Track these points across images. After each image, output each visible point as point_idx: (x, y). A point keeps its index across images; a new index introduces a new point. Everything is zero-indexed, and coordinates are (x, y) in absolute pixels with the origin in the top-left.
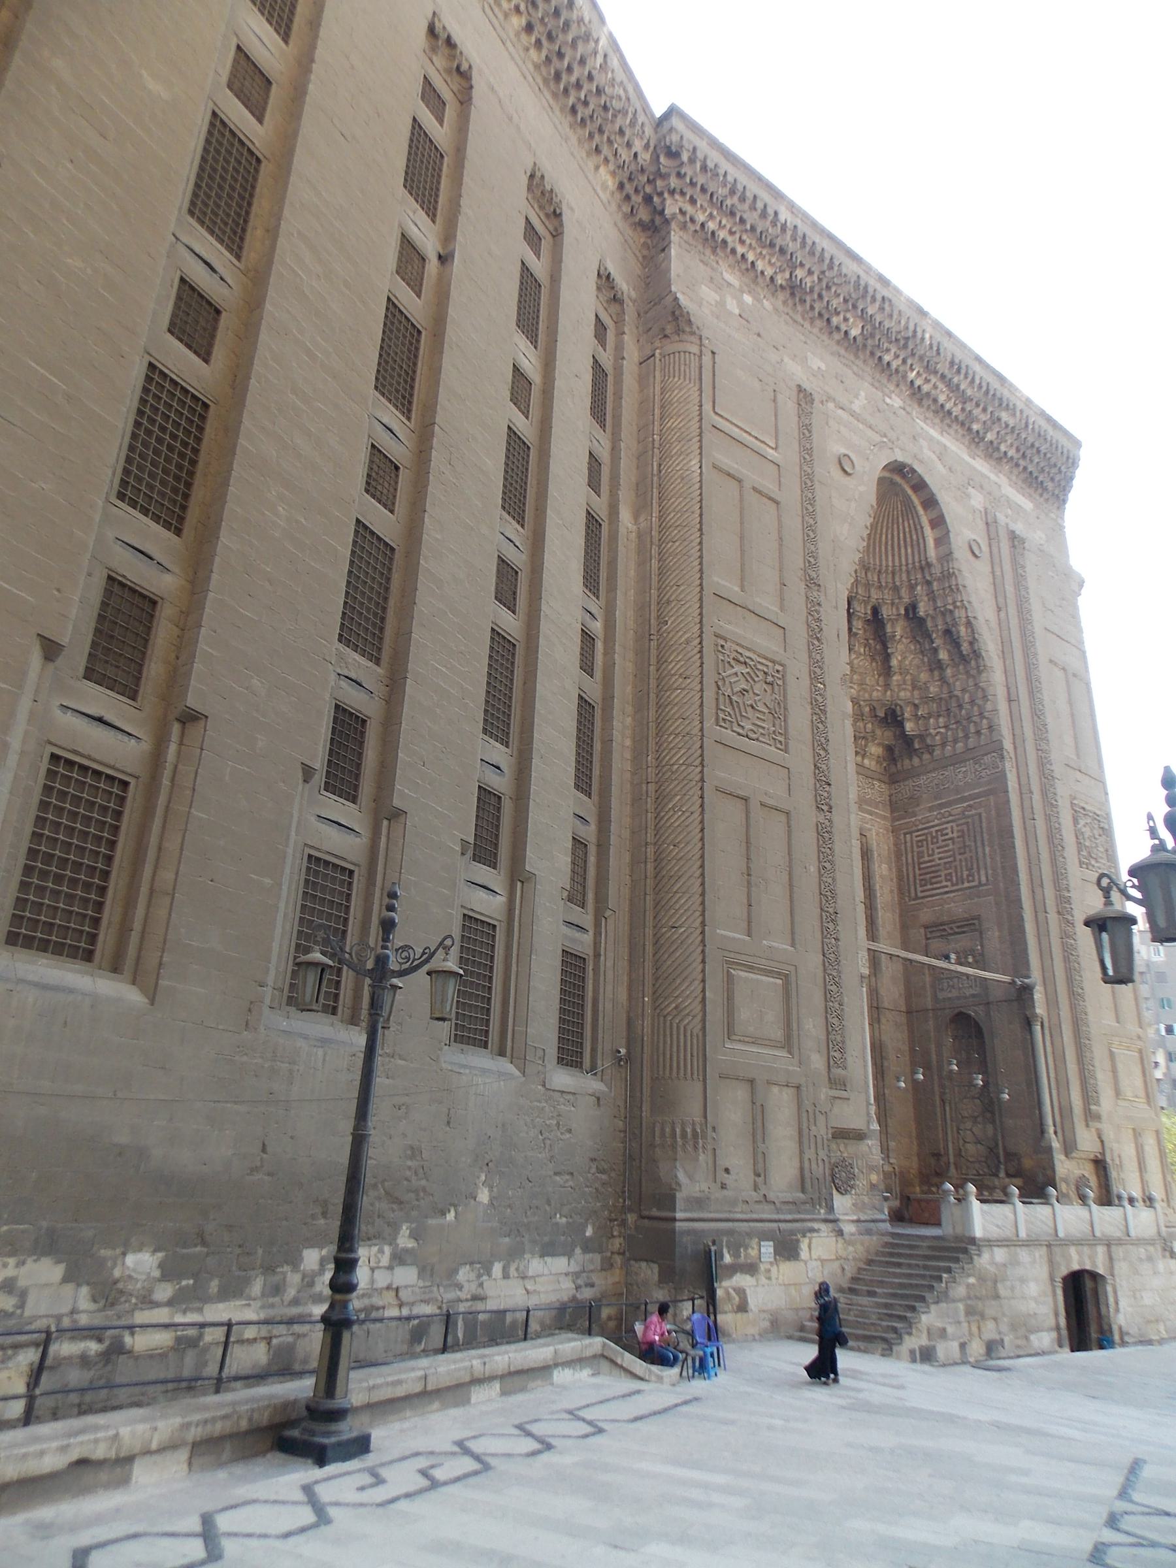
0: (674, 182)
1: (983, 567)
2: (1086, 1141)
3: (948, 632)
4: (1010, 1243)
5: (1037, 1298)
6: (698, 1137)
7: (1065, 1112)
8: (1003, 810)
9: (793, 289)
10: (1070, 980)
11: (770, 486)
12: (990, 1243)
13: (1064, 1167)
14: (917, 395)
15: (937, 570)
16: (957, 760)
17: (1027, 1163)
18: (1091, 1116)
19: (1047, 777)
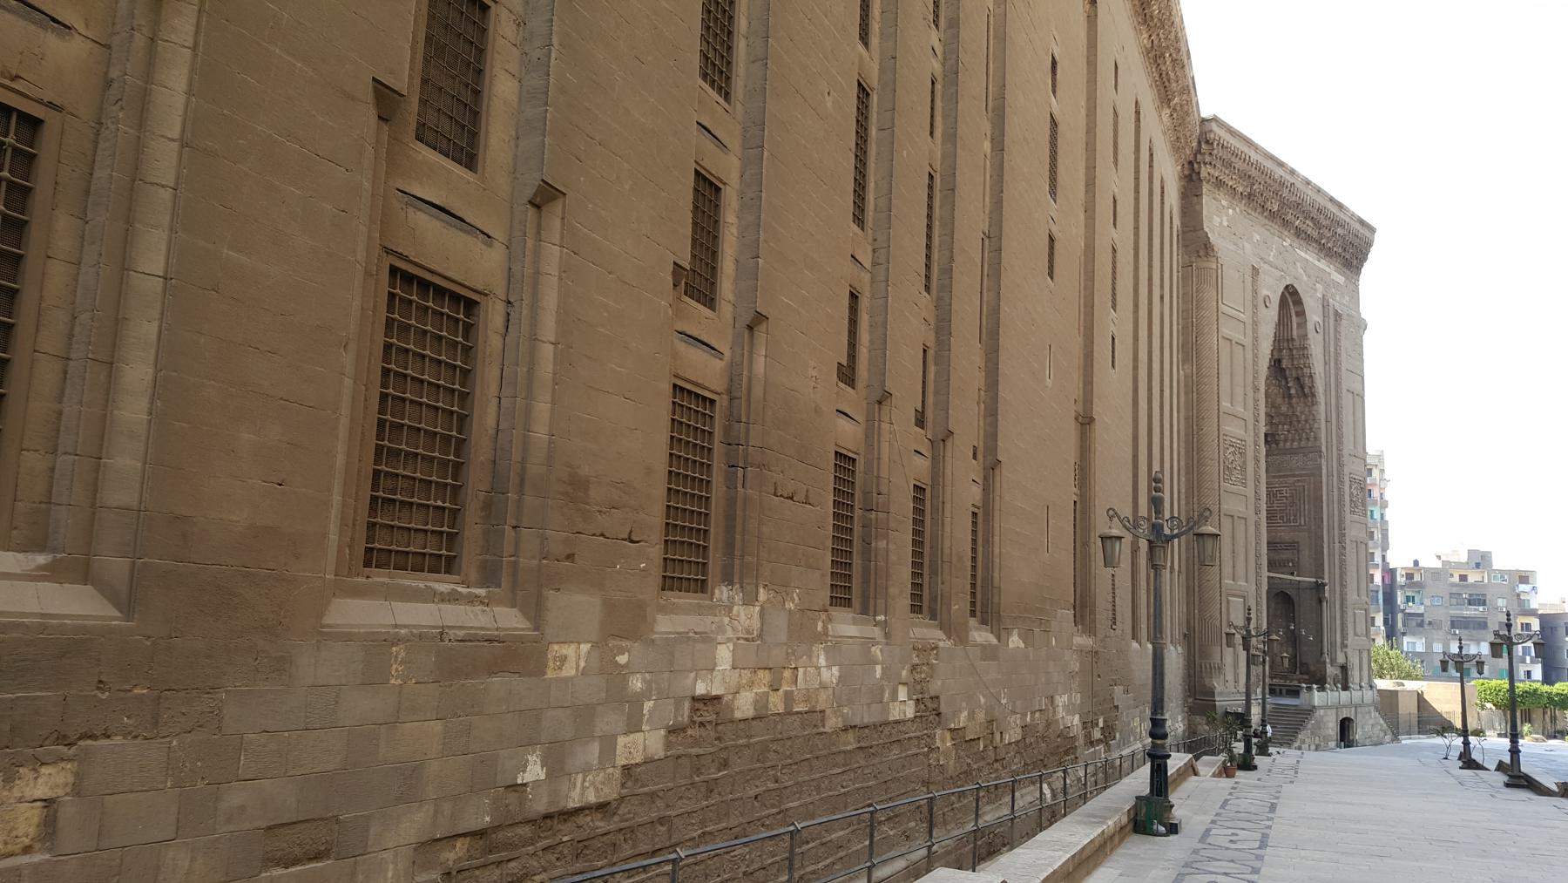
0: (1208, 159)
1: (1320, 337)
2: (1341, 659)
3: (1298, 379)
4: (1327, 707)
5: (1332, 728)
6: (1220, 669)
7: (1333, 644)
8: (1318, 486)
9: (1250, 197)
10: (1341, 578)
11: (1239, 337)
12: (1321, 707)
13: (1331, 671)
14: (1299, 233)
15: (1297, 343)
16: (1294, 452)
17: (1312, 668)
18: (1344, 646)
19: (1341, 465)
